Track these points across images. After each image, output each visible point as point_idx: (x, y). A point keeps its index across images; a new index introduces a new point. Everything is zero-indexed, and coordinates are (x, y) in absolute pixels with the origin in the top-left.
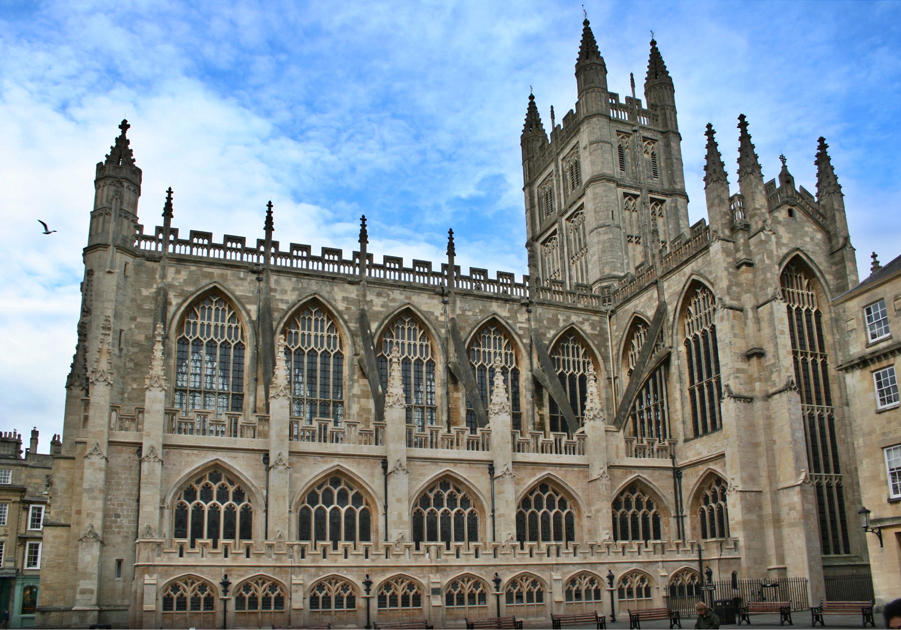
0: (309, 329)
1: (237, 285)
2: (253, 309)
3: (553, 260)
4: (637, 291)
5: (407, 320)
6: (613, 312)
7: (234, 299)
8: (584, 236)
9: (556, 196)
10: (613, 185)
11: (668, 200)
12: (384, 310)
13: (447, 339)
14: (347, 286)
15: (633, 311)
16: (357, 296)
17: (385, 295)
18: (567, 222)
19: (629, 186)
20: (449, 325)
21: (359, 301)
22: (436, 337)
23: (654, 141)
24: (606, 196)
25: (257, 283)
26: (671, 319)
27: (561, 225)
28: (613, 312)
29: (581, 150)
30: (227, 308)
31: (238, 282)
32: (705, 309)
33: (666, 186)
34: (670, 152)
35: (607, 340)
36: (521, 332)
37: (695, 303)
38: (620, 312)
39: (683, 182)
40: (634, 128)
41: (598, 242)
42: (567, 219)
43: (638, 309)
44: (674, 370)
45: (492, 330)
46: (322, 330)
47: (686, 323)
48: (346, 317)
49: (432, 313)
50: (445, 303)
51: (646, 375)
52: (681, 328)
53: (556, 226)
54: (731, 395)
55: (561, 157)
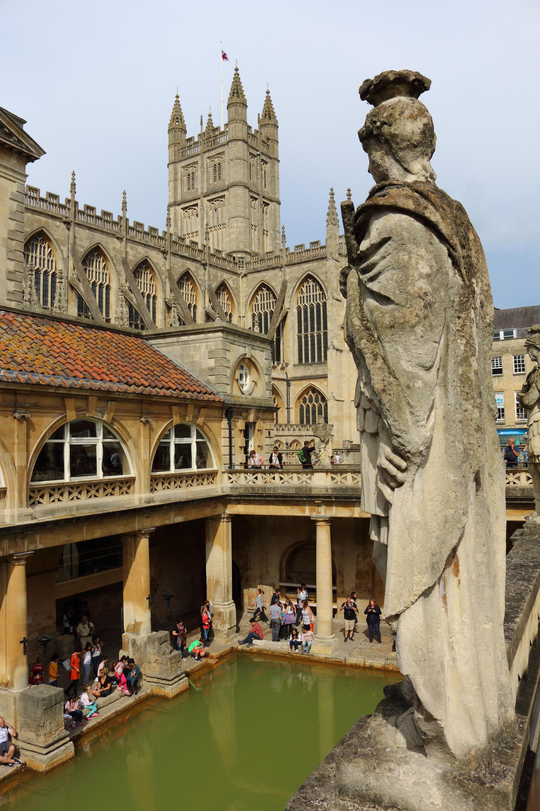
0: (92, 267)
1: (55, 231)
2: (64, 249)
3: (191, 223)
4: (266, 268)
5: (144, 267)
6: (245, 275)
7: (53, 241)
8: (222, 217)
9: (199, 181)
10: (247, 191)
11: (271, 204)
12: (134, 259)
13: (165, 283)
14: (115, 240)
15: (261, 279)
16: (121, 247)
17: (135, 249)
18: (208, 202)
19: (254, 192)
20: (167, 274)
21: (122, 252)
22: (160, 281)
23: (266, 163)
24: (244, 197)
25: (67, 231)
26: (290, 292)
27: (202, 203)
28: (245, 275)
29: (226, 157)
30: (47, 246)
31: (56, 228)
32: (313, 292)
33: (270, 195)
34: (274, 172)
35: (239, 292)
36: (200, 282)
37: (307, 287)
38: (250, 276)
39: (278, 193)
40: (258, 153)
41: (237, 227)
42: (208, 200)
43: (265, 279)
44: (288, 321)
45: (185, 278)
46: (99, 269)
47: (299, 296)
48: (115, 262)
49: (158, 264)
50: (165, 258)
51: (277, 324)
52: (296, 299)
53: (198, 202)
54: (334, 348)
55: (207, 155)
